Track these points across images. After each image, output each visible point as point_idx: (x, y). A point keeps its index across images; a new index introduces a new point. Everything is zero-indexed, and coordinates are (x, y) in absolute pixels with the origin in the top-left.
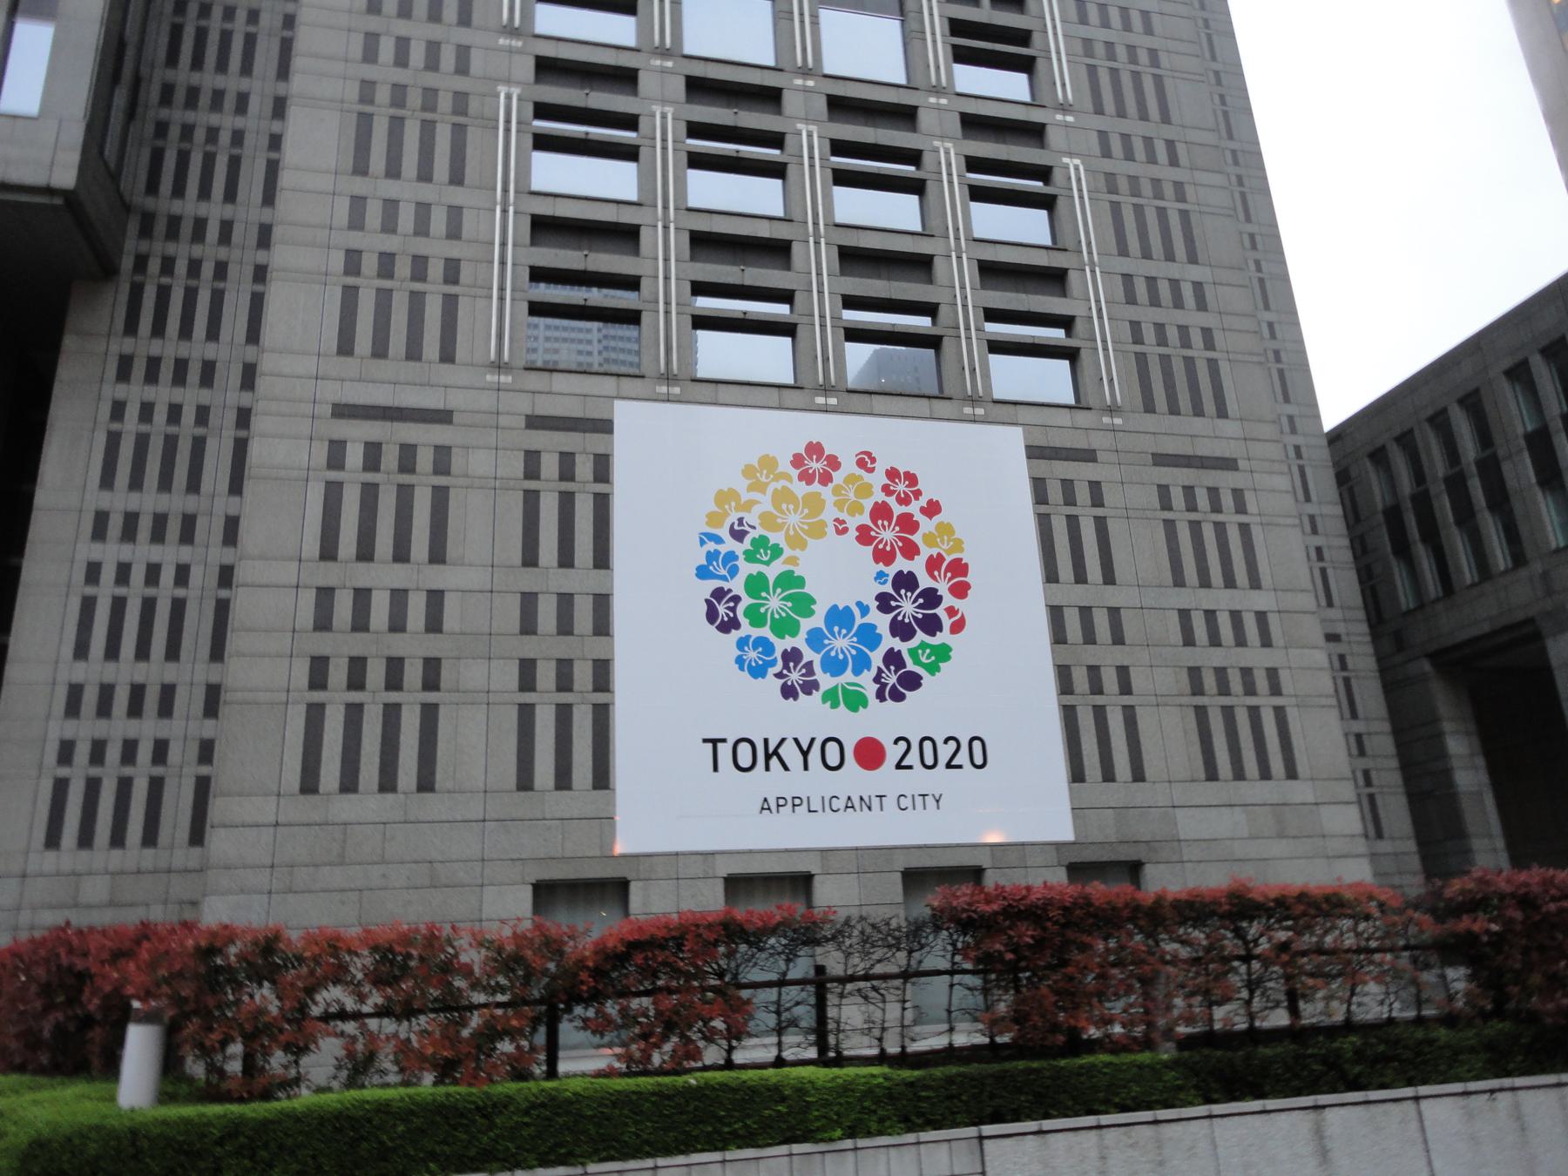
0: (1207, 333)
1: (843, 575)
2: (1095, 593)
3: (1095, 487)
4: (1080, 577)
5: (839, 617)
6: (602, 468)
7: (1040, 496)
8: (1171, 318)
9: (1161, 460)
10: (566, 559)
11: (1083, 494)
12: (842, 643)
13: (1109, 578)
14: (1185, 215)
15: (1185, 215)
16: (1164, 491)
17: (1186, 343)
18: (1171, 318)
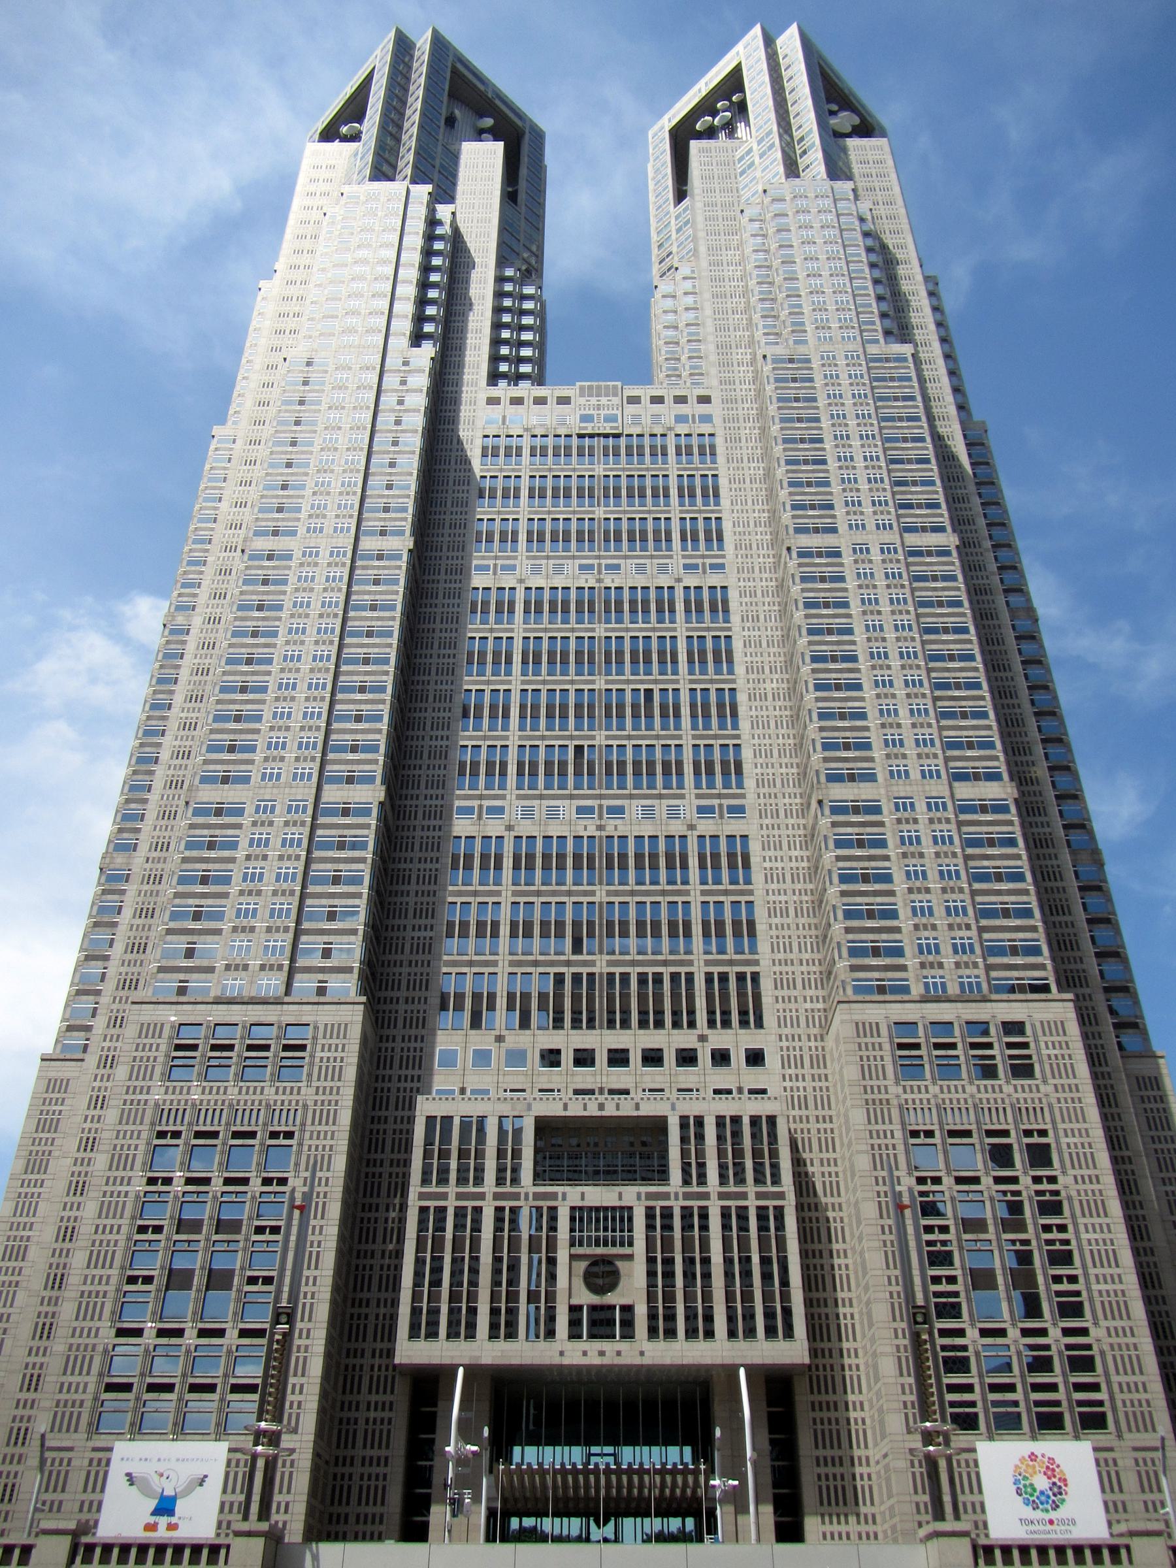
0: (1148, 1401)
1: (1041, 1483)
2: (1118, 1497)
3: (1115, 1461)
4: (1112, 1491)
5: (1042, 1493)
6: (976, 1462)
7: (1097, 1461)
8: (1136, 1396)
9: (1136, 1449)
10: (972, 1492)
11: (1111, 1462)
12: (1043, 1498)
13: (1121, 1490)
14: (1138, 1357)
15: (1138, 1357)
16: (1136, 1460)
17: (1140, 1405)
18: (1136, 1396)
